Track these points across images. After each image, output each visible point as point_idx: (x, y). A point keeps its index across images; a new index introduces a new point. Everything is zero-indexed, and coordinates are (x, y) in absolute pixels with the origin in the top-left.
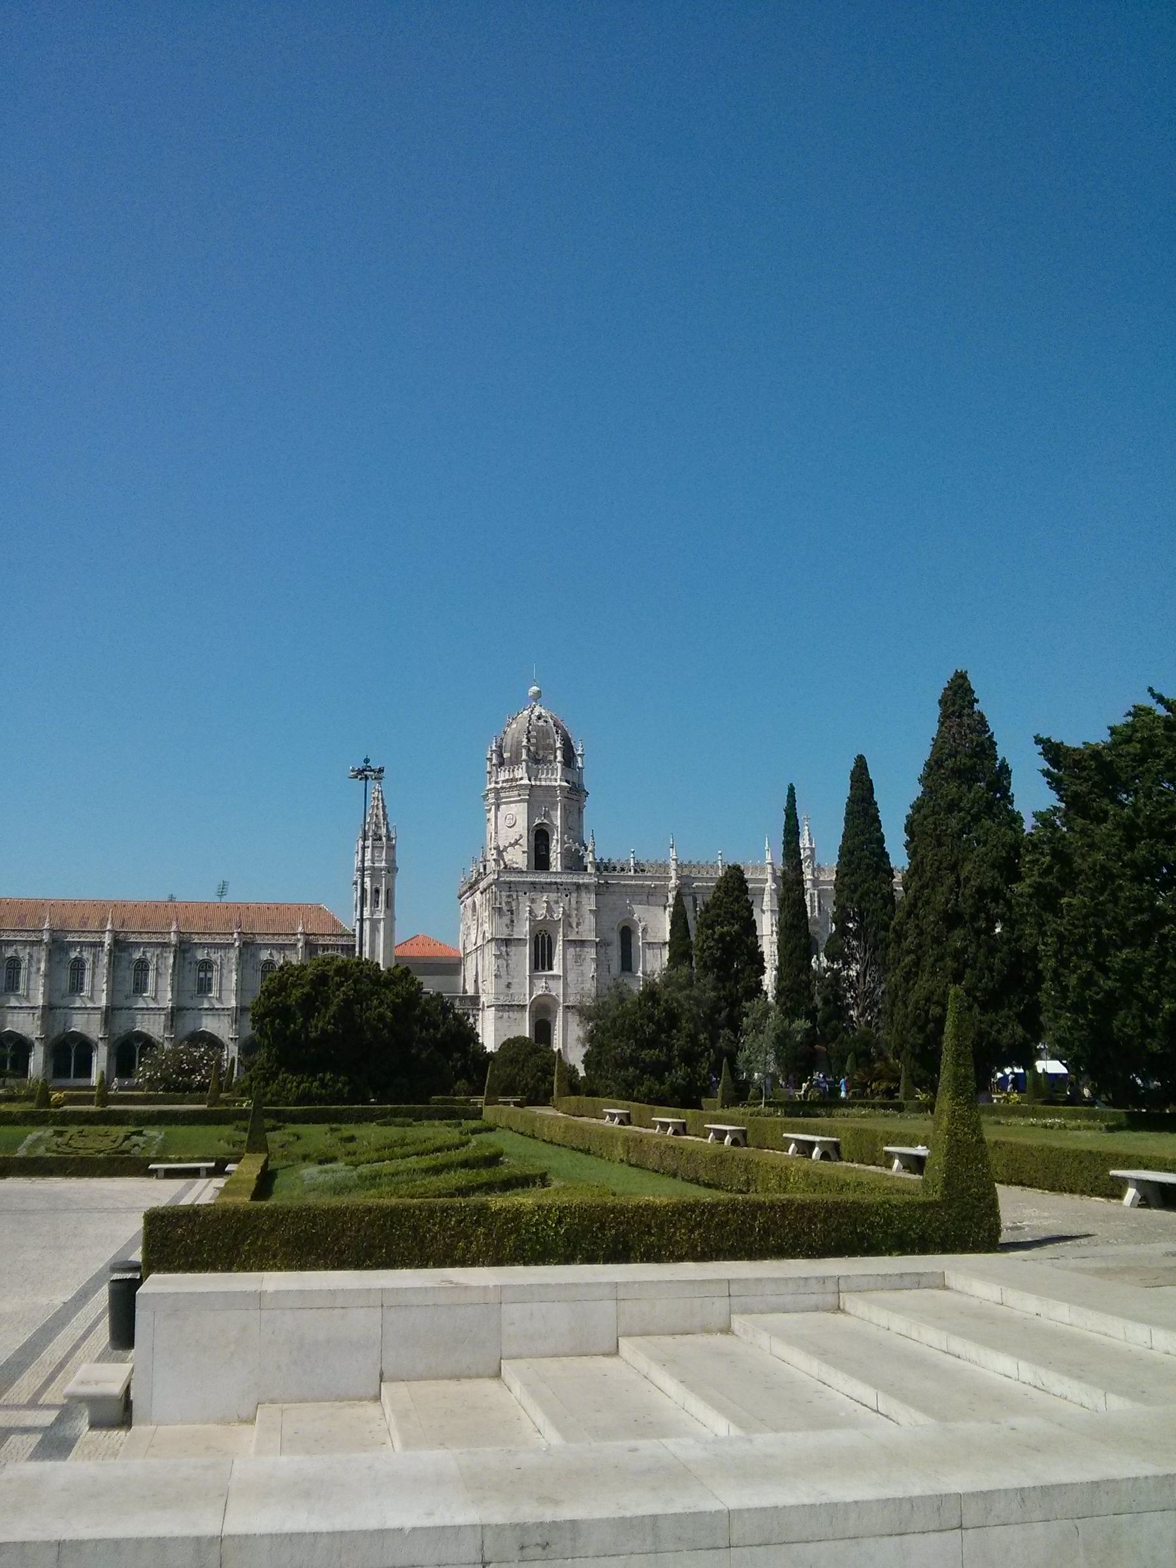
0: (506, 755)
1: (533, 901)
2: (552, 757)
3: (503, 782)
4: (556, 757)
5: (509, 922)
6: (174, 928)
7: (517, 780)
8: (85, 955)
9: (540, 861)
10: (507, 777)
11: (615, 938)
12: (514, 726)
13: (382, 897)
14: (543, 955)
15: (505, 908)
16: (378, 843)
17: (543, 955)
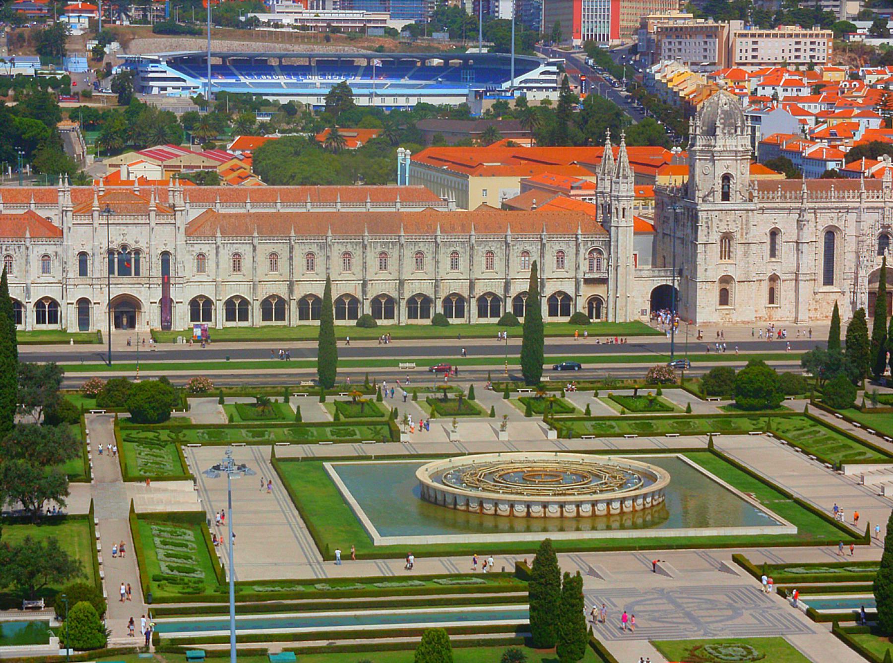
0: (704, 128)
1: (721, 221)
2: (733, 131)
3: (703, 146)
4: (736, 131)
5: (706, 233)
6: (509, 232)
7: (711, 146)
8: (458, 249)
9: (726, 196)
10: (704, 143)
11: (767, 239)
12: (709, 109)
13: (625, 213)
14: (725, 251)
15: (704, 225)
16: (625, 181)
17: (725, 251)
